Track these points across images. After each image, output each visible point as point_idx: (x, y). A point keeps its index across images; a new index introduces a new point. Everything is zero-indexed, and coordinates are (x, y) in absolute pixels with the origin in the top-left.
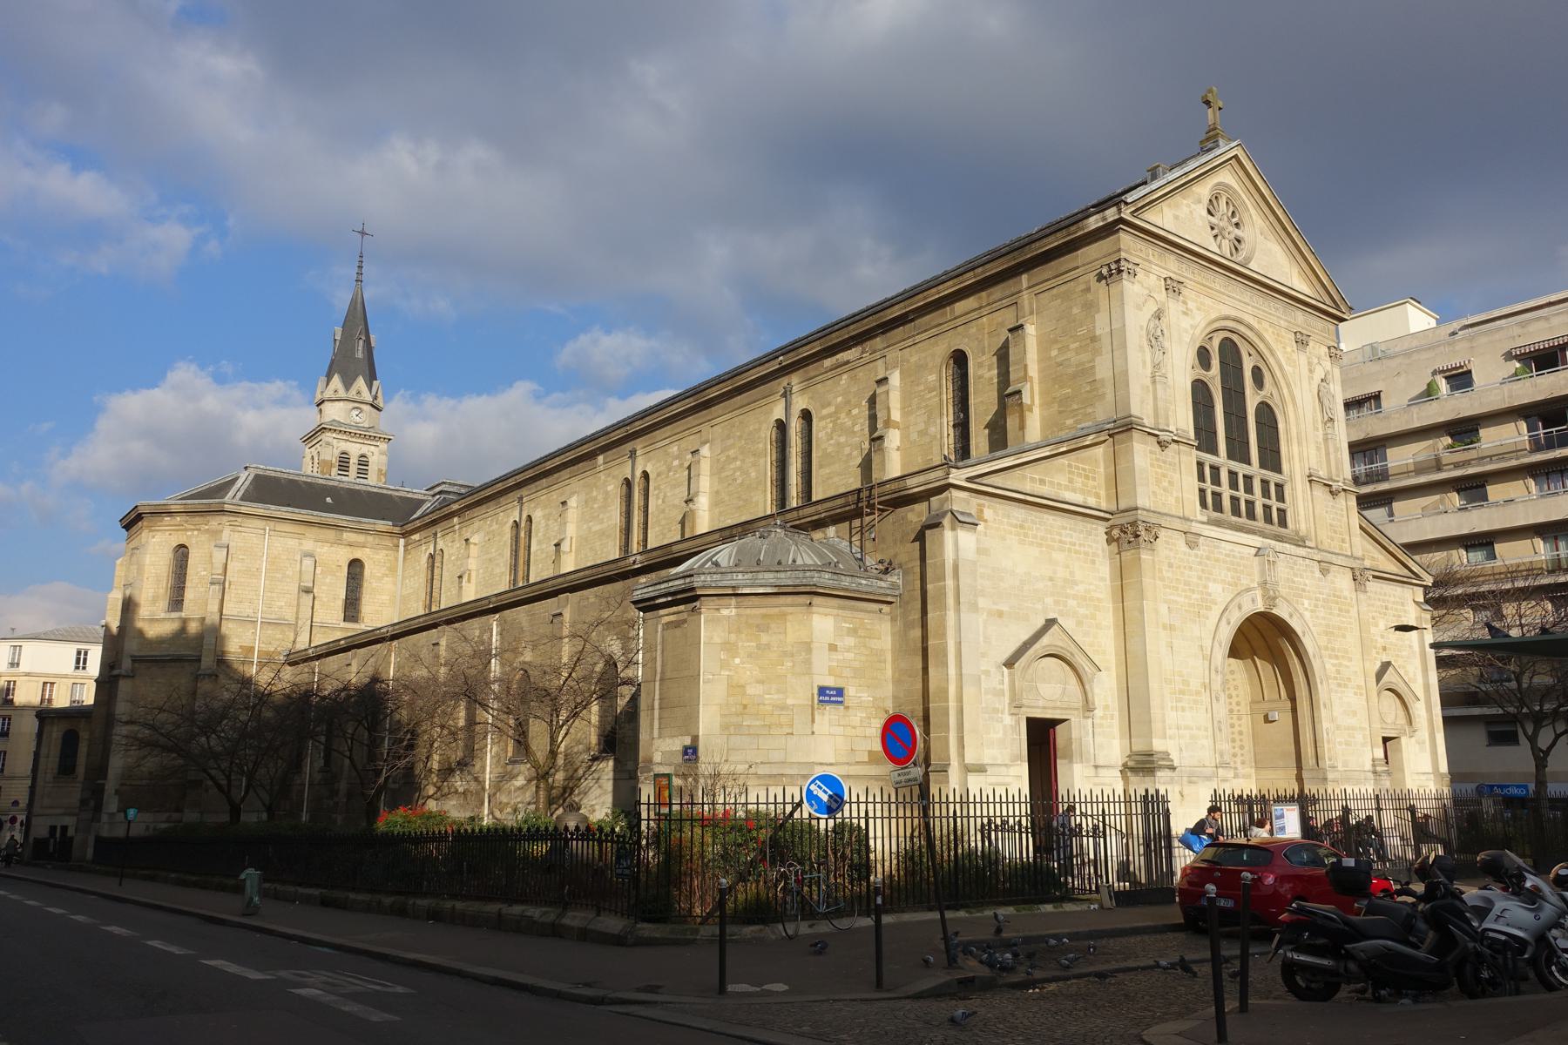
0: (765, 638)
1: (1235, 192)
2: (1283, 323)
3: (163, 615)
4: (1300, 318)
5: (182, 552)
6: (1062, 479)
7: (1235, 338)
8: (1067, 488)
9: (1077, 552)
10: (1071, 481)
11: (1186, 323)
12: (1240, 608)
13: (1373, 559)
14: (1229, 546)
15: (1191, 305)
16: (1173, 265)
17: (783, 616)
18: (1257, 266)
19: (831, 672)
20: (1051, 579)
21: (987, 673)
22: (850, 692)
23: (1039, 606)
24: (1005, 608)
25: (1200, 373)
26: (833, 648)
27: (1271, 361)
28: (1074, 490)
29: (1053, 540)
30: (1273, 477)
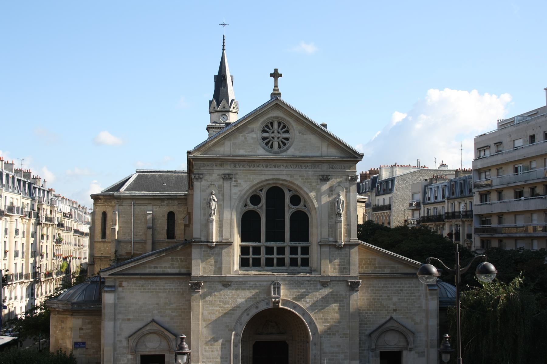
0: (63, 325)
1: (281, 118)
3: (100, 240)
4: (325, 169)
5: (104, 214)
6: (167, 265)
8: (169, 268)
9: (172, 292)
10: (172, 265)
11: (235, 190)
12: (257, 308)
13: (394, 268)
14: (252, 283)
15: (239, 181)
17: (67, 318)
18: (292, 152)
19: (80, 337)
20: (157, 304)
21: (121, 341)
22: (89, 343)
23: (150, 315)
24: (131, 317)
25: (251, 207)
26: (81, 329)
27: (301, 192)
28: (174, 268)
29: (160, 289)
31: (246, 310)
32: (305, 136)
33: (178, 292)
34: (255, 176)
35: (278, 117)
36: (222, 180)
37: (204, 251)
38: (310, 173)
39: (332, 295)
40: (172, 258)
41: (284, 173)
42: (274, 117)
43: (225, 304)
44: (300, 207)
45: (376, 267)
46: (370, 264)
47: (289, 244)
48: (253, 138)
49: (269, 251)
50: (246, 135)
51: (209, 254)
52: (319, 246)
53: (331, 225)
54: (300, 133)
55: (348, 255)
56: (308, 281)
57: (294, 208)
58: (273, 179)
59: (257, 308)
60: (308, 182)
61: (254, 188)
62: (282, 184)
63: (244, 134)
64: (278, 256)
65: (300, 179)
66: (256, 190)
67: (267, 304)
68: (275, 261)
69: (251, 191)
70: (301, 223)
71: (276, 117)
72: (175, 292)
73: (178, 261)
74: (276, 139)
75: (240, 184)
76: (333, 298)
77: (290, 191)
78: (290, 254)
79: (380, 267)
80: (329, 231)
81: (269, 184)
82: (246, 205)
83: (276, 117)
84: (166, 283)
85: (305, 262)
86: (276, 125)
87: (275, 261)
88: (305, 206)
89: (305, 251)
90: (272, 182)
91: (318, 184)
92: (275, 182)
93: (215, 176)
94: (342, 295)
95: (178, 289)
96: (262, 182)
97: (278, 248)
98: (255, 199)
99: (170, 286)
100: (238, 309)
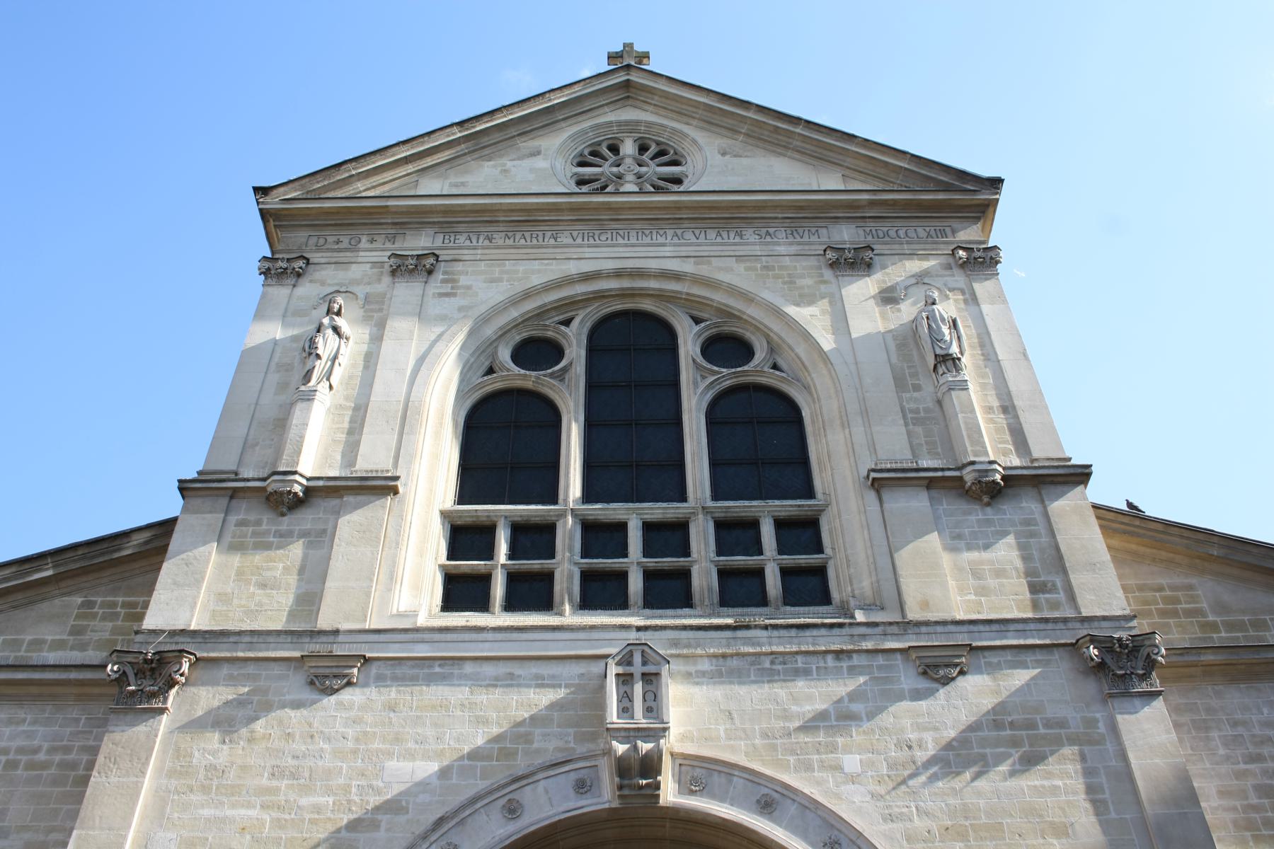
1: (649, 124)
2: (782, 249)
4: (846, 234)
6: (50, 633)
7: (647, 305)
8: (59, 645)
9: (31, 766)
10: (76, 631)
12: (513, 810)
15: (463, 280)
16: (419, 242)
27: (752, 312)
28: (82, 647)
30: (767, 512)
31: (441, 821)
32: (745, 161)
33: (63, 765)
34: (536, 265)
35: (638, 122)
36: (387, 279)
37: (240, 524)
38: (782, 249)
39: (997, 725)
40: (89, 604)
41: (667, 251)
42: (619, 123)
43: (306, 790)
44: (757, 370)
45: (1213, 627)
46: (1175, 614)
47: (710, 503)
48: (532, 170)
49: (603, 537)
50: (509, 164)
51: (267, 533)
52: (871, 496)
53: (917, 411)
54: (724, 154)
55: (1041, 528)
56: (839, 654)
57: (727, 376)
58: (618, 274)
59: (513, 810)
60: (776, 277)
61: (530, 305)
62: (660, 296)
63: (503, 160)
64: (652, 562)
65: (740, 268)
66: (542, 313)
67: (582, 787)
68: (635, 584)
69: (514, 313)
70: (766, 435)
71: (627, 123)
72: (44, 766)
73: (114, 616)
74: (630, 177)
75: (469, 287)
76: (1015, 743)
77: (697, 321)
78: (719, 553)
79: (1231, 626)
80: (909, 434)
81: (600, 296)
82: (490, 371)
83: (630, 127)
84: (10, 722)
85: (809, 586)
86: (628, 148)
87: (635, 584)
88: (775, 367)
89: (803, 532)
90: (613, 284)
91: (825, 282)
92: (626, 283)
93: (356, 271)
94: (1062, 724)
95: (67, 750)
96: (568, 281)
97: (648, 527)
98: (537, 351)
99: (30, 735)
100: (384, 818)
